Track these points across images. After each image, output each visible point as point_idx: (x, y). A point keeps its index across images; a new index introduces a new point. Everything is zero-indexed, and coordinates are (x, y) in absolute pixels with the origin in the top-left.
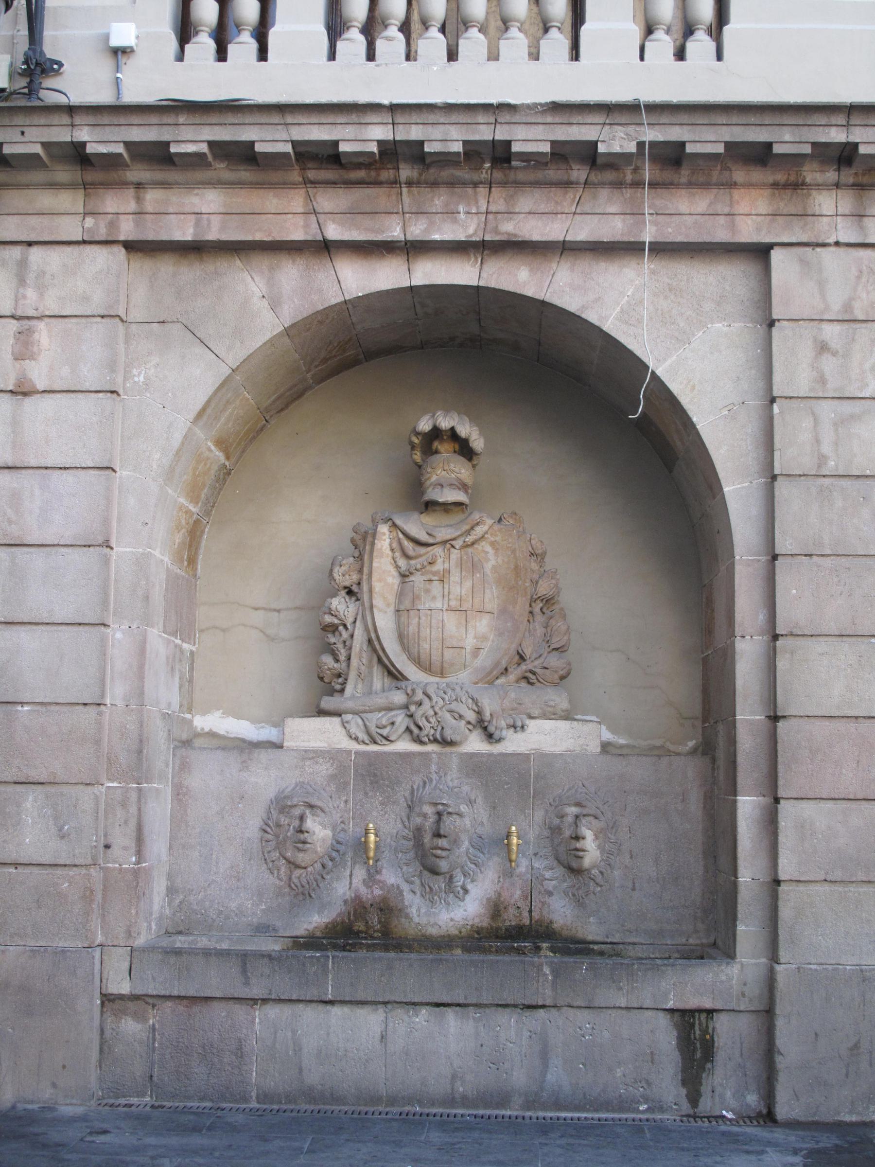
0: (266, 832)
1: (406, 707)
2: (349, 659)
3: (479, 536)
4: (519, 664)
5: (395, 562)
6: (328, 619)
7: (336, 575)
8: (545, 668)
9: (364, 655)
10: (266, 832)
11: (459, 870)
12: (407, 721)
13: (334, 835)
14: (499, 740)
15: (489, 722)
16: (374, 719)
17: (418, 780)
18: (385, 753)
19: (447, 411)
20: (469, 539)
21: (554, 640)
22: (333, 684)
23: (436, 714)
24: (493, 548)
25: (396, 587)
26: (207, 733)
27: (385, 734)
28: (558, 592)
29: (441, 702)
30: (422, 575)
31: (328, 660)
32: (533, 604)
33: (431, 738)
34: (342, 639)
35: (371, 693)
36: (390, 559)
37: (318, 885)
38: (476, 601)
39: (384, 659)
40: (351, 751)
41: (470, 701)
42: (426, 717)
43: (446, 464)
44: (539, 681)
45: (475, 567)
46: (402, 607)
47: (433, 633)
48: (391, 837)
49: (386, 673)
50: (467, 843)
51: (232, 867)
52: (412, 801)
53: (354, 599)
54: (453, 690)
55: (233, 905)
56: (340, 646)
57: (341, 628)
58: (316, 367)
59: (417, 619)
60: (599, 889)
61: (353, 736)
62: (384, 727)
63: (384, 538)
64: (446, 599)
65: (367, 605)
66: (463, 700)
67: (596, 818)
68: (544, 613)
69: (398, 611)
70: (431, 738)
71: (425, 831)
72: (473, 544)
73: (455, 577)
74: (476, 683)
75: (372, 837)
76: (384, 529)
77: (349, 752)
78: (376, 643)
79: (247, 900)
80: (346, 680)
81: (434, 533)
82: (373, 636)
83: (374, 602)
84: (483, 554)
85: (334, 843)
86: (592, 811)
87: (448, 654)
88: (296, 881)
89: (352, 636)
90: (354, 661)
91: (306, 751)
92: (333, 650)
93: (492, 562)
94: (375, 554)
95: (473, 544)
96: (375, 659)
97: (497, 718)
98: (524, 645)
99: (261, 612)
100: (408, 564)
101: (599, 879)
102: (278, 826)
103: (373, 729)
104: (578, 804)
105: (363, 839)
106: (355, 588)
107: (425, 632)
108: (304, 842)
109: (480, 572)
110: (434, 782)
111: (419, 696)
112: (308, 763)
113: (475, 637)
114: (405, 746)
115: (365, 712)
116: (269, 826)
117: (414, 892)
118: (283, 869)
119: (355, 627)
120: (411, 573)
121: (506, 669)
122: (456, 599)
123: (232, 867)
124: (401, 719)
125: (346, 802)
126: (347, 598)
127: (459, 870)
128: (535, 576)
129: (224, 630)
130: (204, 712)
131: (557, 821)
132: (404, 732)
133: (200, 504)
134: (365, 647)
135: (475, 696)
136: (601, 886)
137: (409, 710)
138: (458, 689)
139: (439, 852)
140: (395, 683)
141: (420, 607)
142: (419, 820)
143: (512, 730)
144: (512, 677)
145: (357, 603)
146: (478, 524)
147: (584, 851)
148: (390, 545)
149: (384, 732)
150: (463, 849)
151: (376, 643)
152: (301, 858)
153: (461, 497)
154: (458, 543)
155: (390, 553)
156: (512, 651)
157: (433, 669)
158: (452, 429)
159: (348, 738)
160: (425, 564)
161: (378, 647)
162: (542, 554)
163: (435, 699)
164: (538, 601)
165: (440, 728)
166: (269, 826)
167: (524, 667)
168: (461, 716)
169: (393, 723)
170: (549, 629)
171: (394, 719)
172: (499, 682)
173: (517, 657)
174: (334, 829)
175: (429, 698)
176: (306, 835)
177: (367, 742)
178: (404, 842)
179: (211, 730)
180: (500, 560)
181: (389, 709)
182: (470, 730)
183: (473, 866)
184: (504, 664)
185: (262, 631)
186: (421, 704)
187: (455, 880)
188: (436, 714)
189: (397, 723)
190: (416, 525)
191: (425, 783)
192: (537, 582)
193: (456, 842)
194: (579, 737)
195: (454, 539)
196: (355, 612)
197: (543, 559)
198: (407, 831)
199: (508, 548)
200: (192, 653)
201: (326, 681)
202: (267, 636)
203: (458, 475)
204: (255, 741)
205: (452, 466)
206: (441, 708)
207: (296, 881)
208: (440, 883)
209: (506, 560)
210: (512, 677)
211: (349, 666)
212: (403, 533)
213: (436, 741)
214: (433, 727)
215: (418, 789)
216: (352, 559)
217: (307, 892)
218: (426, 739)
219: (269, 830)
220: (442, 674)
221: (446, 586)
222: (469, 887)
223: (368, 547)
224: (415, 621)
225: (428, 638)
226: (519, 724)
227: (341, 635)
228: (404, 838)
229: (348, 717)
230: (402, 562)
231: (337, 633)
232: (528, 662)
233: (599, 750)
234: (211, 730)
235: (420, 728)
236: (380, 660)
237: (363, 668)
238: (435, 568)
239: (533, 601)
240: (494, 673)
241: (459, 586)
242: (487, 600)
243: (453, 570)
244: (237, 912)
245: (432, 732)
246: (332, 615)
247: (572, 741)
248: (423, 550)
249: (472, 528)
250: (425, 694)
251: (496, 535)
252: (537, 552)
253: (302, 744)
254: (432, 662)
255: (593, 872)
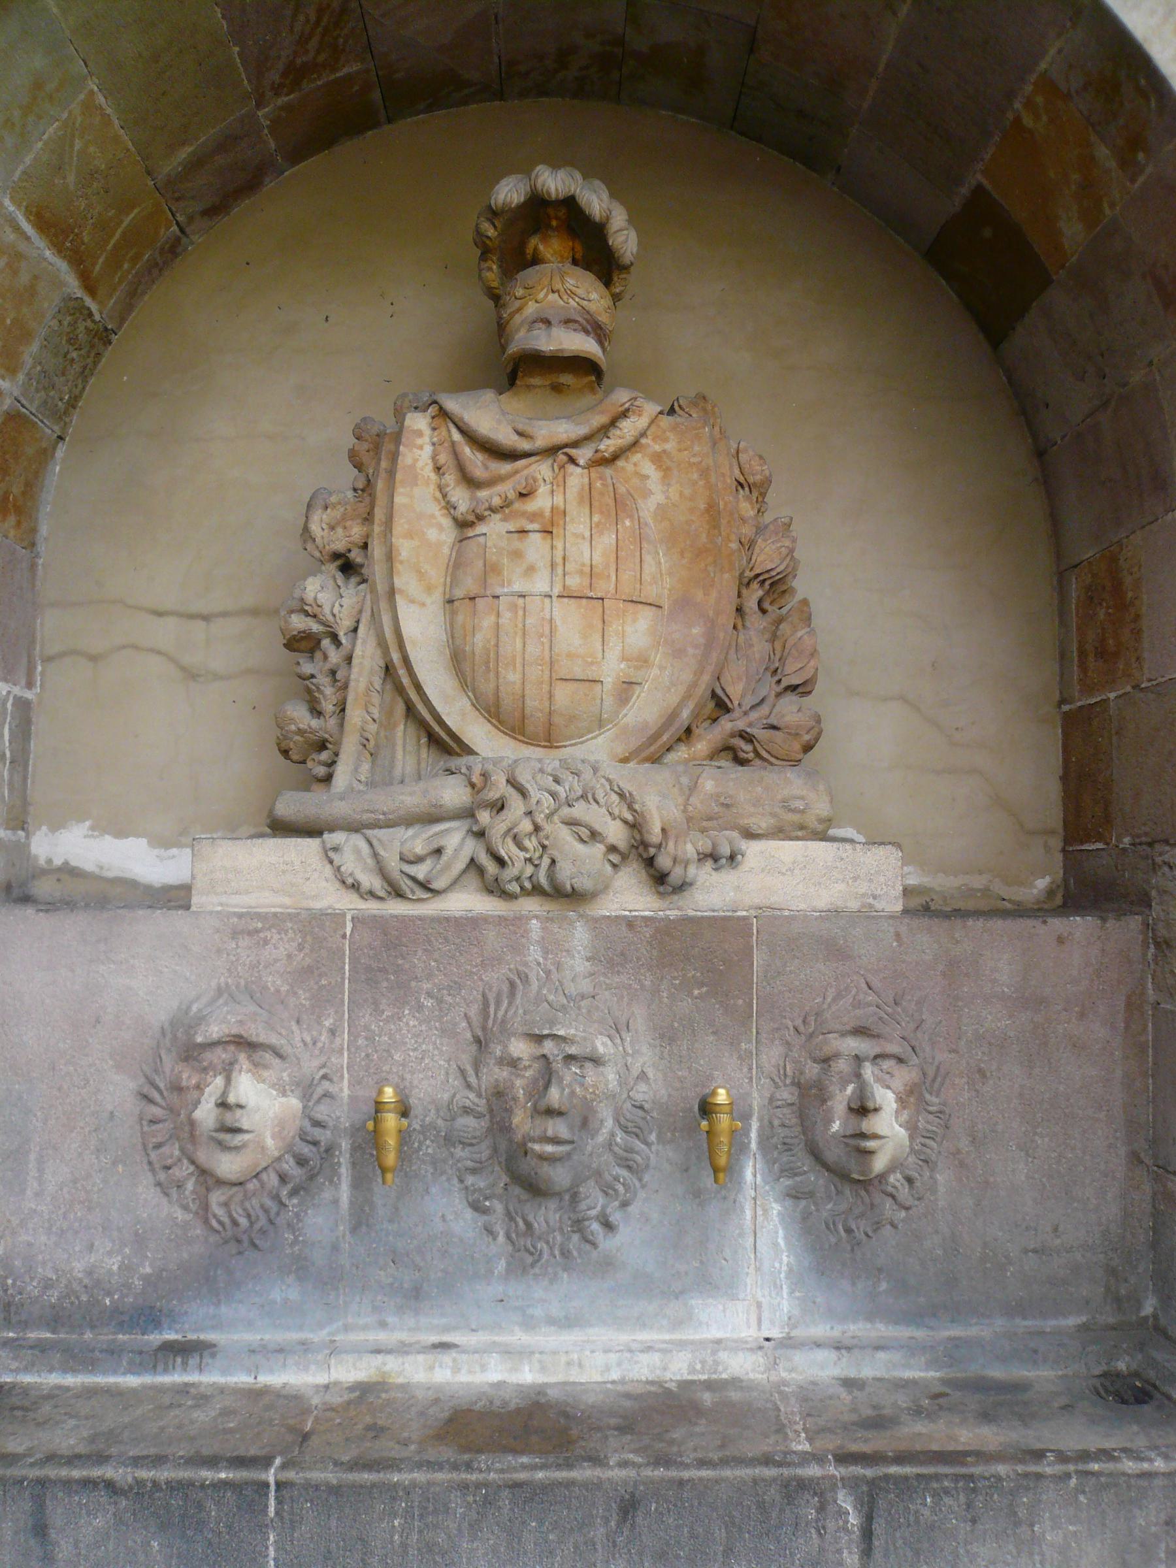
0: (150, 1101)
1: (468, 814)
2: (343, 710)
3: (629, 439)
4: (715, 720)
5: (445, 496)
6: (298, 623)
7: (315, 528)
8: (774, 728)
9: (376, 699)
10: (150, 1101)
11: (591, 1183)
12: (471, 847)
13: (304, 1107)
14: (682, 887)
15: (659, 846)
16: (400, 842)
17: (495, 977)
18: (420, 918)
19: (555, 166)
20: (608, 446)
21: (790, 667)
22: (310, 764)
23: (537, 829)
24: (659, 468)
25: (446, 550)
26: (60, 869)
27: (421, 877)
28: (795, 569)
29: (547, 801)
30: (505, 520)
31: (299, 714)
32: (744, 591)
33: (528, 885)
34: (328, 666)
35: (392, 784)
36: (432, 488)
37: (271, 1222)
38: (626, 576)
39: (420, 707)
40: (344, 915)
41: (615, 798)
42: (515, 837)
43: (557, 279)
44: (758, 755)
45: (620, 506)
46: (459, 593)
47: (530, 649)
48: (438, 1110)
49: (424, 740)
50: (609, 1123)
51: (75, 1181)
52: (484, 1028)
53: (354, 580)
54: (577, 774)
55: (78, 1267)
56: (323, 680)
57: (326, 643)
58: (277, 90)
59: (493, 618)
60: (903, 1214)
61: (350, 881)
62: (419, 860)
63: (419, 441)
64: (560, 571)
65: (381, 587)
66: (600, 796)
67: (900, 1060)
68: (764, 611)
69: (450, 601)
70: (528, 885)
71: (515, 1099)
72: (615, 458)
73: (579, 523)
74: (625, 760)
75: (391, 1121)
76: (419, 422)
77: (337, 918)
78: (402, 672)
79: (110, 1253)
80: (337, 755)
81: (528, 429)
82: (396, 656)
83: (396, 580)
84: (635, 481)
85: (307, 1124)
86: (893, 1048)
87: (563, 694)
88: (220, 1212)
89: (349, 659)
90: (355, 715)
91: (240, 916)
92: (309, 691)
93: (657, 498)
94: (399, 476)
95: (615, 458)
96: (400, 708)
97: (677, 837)
98: (726, 679)
99: (171, 621)
100: (473, 498)
101: (904, 1193)
102: (178, 1089)
103: (394, 865)
104: (860, 1031)
105: (370, 1125)
106: (356, 556)
107: (511, 645)
108: (238, 1131)
109: (631, 517)
110: (535, 985)
111: (500, 788)
112: (245, 942)
113: (624, 658)
114: (467, 901)
115: (376, 825)
116: (157, 1088)
117: (489, 1231)
118: (190, 1186)
119: (355, 638)
120: (480, 518)
121: (688, 731)
122: (581, 572)
123: (75, 1181)
124: (456, 840)
125: (333, 1032)
126: (339, 575)
127: (591, 1183)
128: (747, 531)
129: (94, 658)
130: (56, 826)
131: (812, 1070)
132: (464, 871)
133: (21, 377)
134: (377, 683)
135: (627, 787)
136: (907, 1209)
137: (477, 821)
138: (587, 774)
139: (549, 1148)
140: (444, 762)
141: (498, 591)
142: (502, 1074)
143: (709, 864)
144: (701, 747)
145: (363, 586)
146: (624, 414)
147: (876, 1137)
148: (434, 458)
149: (420, 871)
150: (600, 1139)
151: (402, 672)
152: (228, 1165)
153: (586, 345)
154: (584, 454)
155: (433, 476)
156: (702, 689)
157: (530, 729)
158: (570, 202)
159: (338, 885)
160: (512, 495)
161: (406, 681)
162: (762, 483)
163: (535, 794)
164: (755, 585)
165: (546, 861)
166: (157, 1088)
167: (726, 725)
168: (594, 835)
169: (438, 851)
170: (778, 645)
171: (442, 843)
172: (671, 757)
173: (711, 705)
174: (306, 1097)
175: (523, 792)
176: (239, 1112)
177: (382, 894)
178: (469, 1122)
179: (66, 863)
180: (673, 492)
181: (431, 818)
182: (614, 866)
183: (624, 1173)
184: (685, 714)
185: (171, 659)
186: (502, 808)
187: (583, 1206)
188: (537, 829)
189: (449, 851)
190: (488, 415)
191: (512, 985)
192: (752, 543)
193: (585, 1123)
194: (855, 879)
195: (575, 444)
196: (358, 607)
197: (763, 495)
198: (472, 1096)
199: (691, 465)
200: (23, 706)
201: (295, 757)
202: (183, 669)
203: (585, 303)
204: (157, 885)
205: (570, 282)
206: (549, 817)
207: (220, 1212)
208: (545, 1216)
209: (687, 492)
210: (701, 747)
211: (341, 725)
212: (462, 431)
213: (537, 890)
214: (530, 860)
215: (498, 1004)
216: (350, 494)
217: (245, 1238)
218: (514, 888)
219: (156, 1096)
220: (548, 738)
221: (559, 545)
222: (616, 1217)
223: (384, 464)
224: (487, 622)
225: (519, 660)
226: (726, 850)
227: (326, 657)
228: (466, 1111)
229: (338, 838)
230: (461, 498)
231: (318, 655)
232: (737, 713)
233: (899, 907)
234: (66, 863)
235: (501, 862)
236: (410, 710)
237: (373, 727)
238: (531, 506)
239: (745, 583)
240: (665, 738)
241: (587, 544)
242: (647, 577)
243: (572, 509)
244: (86, 1281)
245: (529, 870)
246: (307, 614)
247: (842, 887)
248: (506, 467)
249: (613, 423)
250: (512, 782)
251: (666, 440)
252: (751, 480)
253: (236, 900)
254: (528, 711)
255: (892, 1179)
